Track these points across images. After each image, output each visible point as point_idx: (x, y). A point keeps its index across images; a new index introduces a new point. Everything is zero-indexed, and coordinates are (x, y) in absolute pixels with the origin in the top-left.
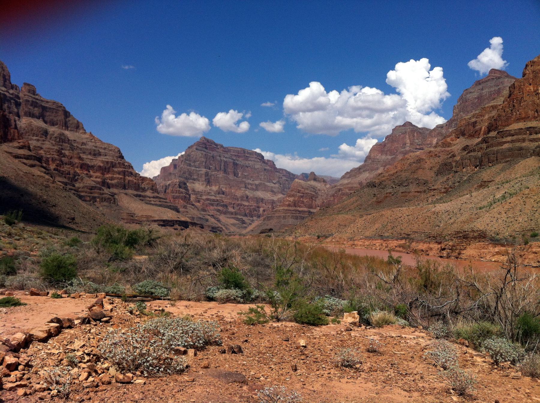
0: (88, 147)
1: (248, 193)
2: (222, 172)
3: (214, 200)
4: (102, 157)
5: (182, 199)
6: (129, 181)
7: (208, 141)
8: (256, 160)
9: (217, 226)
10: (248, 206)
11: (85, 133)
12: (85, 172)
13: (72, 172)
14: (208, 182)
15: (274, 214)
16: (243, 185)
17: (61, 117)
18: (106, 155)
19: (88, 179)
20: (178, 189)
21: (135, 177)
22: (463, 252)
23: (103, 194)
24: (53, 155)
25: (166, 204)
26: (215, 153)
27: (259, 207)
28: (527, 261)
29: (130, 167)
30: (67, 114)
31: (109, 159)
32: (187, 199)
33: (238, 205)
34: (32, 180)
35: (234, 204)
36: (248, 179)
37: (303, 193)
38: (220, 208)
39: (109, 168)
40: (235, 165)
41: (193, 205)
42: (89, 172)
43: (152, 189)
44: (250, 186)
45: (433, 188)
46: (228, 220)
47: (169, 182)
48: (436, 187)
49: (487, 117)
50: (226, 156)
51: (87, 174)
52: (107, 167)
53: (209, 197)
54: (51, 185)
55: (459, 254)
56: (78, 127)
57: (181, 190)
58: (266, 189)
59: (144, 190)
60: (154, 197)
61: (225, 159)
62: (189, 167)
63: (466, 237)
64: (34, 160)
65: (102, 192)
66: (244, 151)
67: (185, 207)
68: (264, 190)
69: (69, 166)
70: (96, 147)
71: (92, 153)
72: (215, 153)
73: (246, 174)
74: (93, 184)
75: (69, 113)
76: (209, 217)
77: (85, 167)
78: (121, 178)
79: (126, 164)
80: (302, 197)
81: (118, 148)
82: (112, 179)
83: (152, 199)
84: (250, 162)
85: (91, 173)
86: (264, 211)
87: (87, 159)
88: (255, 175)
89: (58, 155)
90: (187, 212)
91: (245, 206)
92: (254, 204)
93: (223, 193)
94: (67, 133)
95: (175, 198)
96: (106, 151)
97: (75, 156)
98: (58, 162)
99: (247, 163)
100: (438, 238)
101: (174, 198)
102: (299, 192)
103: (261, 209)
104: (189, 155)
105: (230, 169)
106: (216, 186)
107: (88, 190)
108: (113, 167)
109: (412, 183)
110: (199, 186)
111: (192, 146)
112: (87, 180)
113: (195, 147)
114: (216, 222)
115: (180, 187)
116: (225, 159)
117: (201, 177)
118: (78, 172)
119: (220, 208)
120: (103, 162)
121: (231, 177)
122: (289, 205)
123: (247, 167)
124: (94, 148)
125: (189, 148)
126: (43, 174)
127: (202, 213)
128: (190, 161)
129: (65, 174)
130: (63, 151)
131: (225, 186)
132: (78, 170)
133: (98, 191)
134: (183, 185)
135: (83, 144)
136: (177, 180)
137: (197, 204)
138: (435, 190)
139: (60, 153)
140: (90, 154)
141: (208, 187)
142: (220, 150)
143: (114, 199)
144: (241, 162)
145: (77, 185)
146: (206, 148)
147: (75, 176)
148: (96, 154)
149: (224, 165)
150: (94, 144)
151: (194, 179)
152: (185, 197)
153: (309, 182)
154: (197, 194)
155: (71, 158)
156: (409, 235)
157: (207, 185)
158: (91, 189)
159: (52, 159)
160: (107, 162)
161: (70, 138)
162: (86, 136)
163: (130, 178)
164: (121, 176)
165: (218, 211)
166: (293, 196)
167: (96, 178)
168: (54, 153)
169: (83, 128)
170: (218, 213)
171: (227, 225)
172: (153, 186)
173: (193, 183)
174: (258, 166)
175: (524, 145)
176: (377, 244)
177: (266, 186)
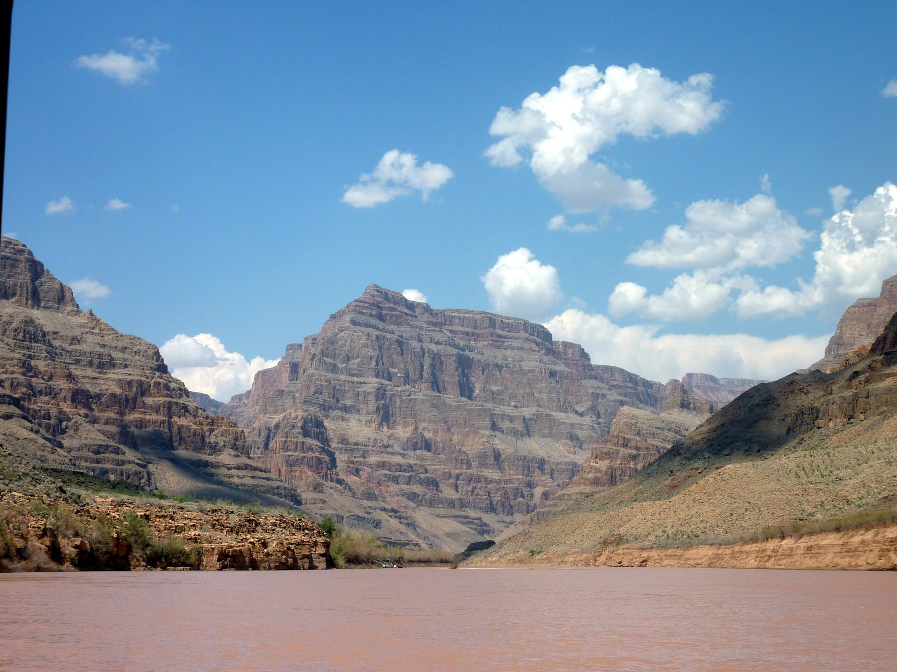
0: (85, 347)
1: (502, 444)
2: (424, 386)
3: (399, 467)
4: (117, 370)
5: (310, 467)
6: (180, 428)
7: (386, 296)
8: (527, 345)
9: (403, 539)
10: (498, 482)
11: (78, 312)
12: (83, 411)
13: (54, 412)
14: (386, 416)
15: (556, 505)
16: (487, 422)
17: (24, 277)
18: (126, 366)
19: (88, 426)
20: (301, 439)
21: (195, 416)
23: (123, 463)
24: (13, 373)
25: (269, 483)
26: (405, 331)
27: (530, 485)
29: (183, 391)
30: (36, 269)
31: (134, 374)
32: (326, 465)
33: (470, 479)
34: (20, 450)
35: (458, 477)
36: (502, 402)
37: (637, 448)
38: (417, 489)
39: (135, 399)
40: (464, 364)
41: (340, 482)
42: (91, 410)
43: (234, 447)
44: (505, 425)
46: (439, 522)
47: (277, 418)
50: (438, 337)
51: (86, 416)
52: (131, 395)
53: (386, 458)
54: (50, 457)
56: (62, 297)
57: (309, 441)
58: (552, 429)
59: (215, 449)
60: (238, 468)
61: (433, 347)
62: (331, 375)
64: (9, 404)
65: (120, 457)
66: (492, 321)
67: (317, 488)
68: (550, 435)
69: (47, 398)
70: (104, 346)
71: (96, 361)
72: (405, 331)
73: (495, 388)
74: (101, 439)
75: (42, 265)
76: (383, 516)
77: (81, 397)
78: (163, 422)
79: (173, 385)
80: (634, 458)
81: (156, 348)
82: (141, 424)
83: (233, 472)
84: (508, 352)
85: (97, 413)
86: (546, 495)
87: (84, 377)
88: (521, 391)
89: (23, 374)
90: (324, 502)
91: (491, 481)
92: (517, 477)
93: (428, 446)
94: (38, 315)
95: (291, 464)
96: (127, 356)
97: (59, 372)
98: (24, 390)
99: (500, 354)
101: (291, 464)
102: (625, 445)
103: (538, 491)
104: (332, 342)
105: (450, 376)
106: (405, 425)
107: (91, 455)
108: (143, 395)
110: (358, 428)
111: (341, 313)
112: (89, 431)
113: (348, 317)
114: (403, 528)
115: (306, 433)
116: (433, 347)
117: (366, 402)
118: (67, 410)
119: (417, 489)
120: (120, 383)
121: (452, 398)
122: (596, 482)
123: (499, 367)
124: (98, 349)
125: (333, 317)
126: (33, 436)
127: (366, 503)
128: (334, 357)
129: (39, 418)
130: (33, 363)
131: (431, 426)
132: (67, 407)
133: (112, 456)
134: (313, 427)
135: (75, 340)
136: (297, 414)
137: (352, 479)
139: (27, 368)
140: (91, 364)
141: (385, 429)
142: (422, 321)
143: (149, 474)
144: (482, 352)
145: (66, 442)
146: (381, 318)
147: (61, 421)
148: (104, 364)
149: (432, 366)
150: (98, 339)
151: (345, 409)
152: (319, 461)
153: (664, 415)
154: (352, 450)
155: (51, 378)
157: (380, 425)
158: (97, 452)
159: (12, 384)
160: (130, 383)
161: (46, 329)
162: (80, 320)
163: (183, 421)
164: (163, 418)
165: (412, 497)
166: (608, 455)
167: (106, 423)
168: (15, 369)
169: (73, 299)
170: (411, 504)
171: (434, 536)
172: (236, 439)
173: (343, 420)
174: (532, 362)
177: (553, 423)
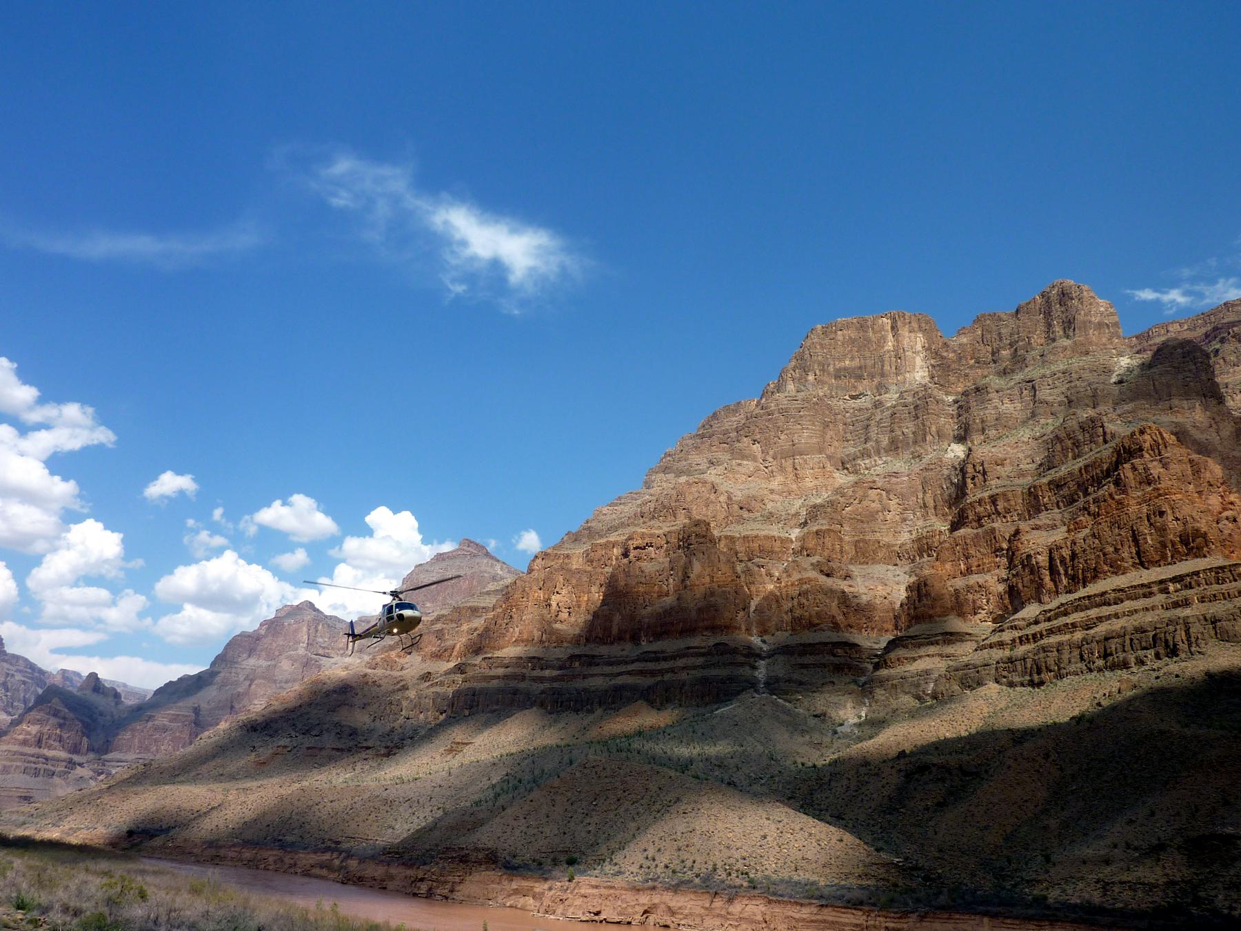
22: (457, 888)
28: (571, 910)
45: (365, 744)
48: (369, 744)
49: (465, 627)
55: (452, 891)
63: (464, 860)
100: (406, 856)
109: (327, 730)
122: (25, 743)
138: (368, 748)
156: (338, 843)
175: (522, 685)
176: (271, 859)
